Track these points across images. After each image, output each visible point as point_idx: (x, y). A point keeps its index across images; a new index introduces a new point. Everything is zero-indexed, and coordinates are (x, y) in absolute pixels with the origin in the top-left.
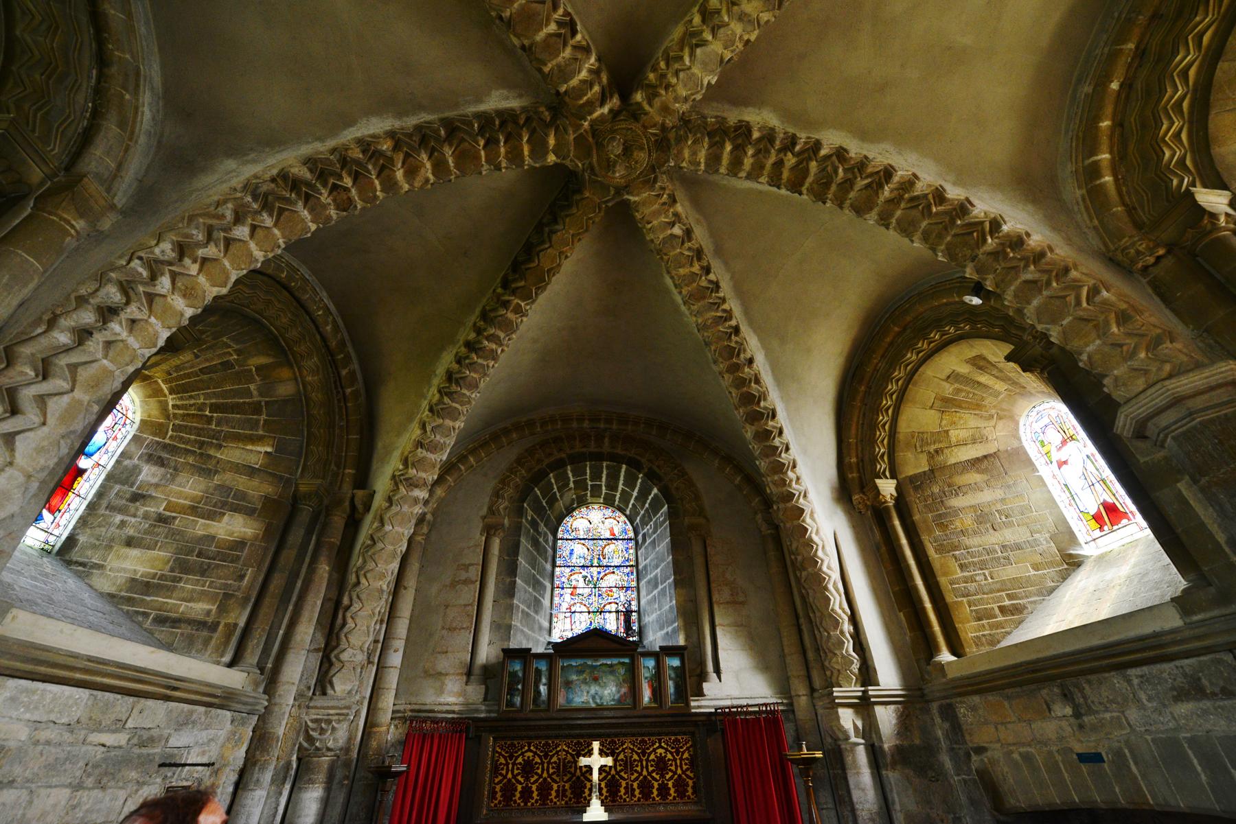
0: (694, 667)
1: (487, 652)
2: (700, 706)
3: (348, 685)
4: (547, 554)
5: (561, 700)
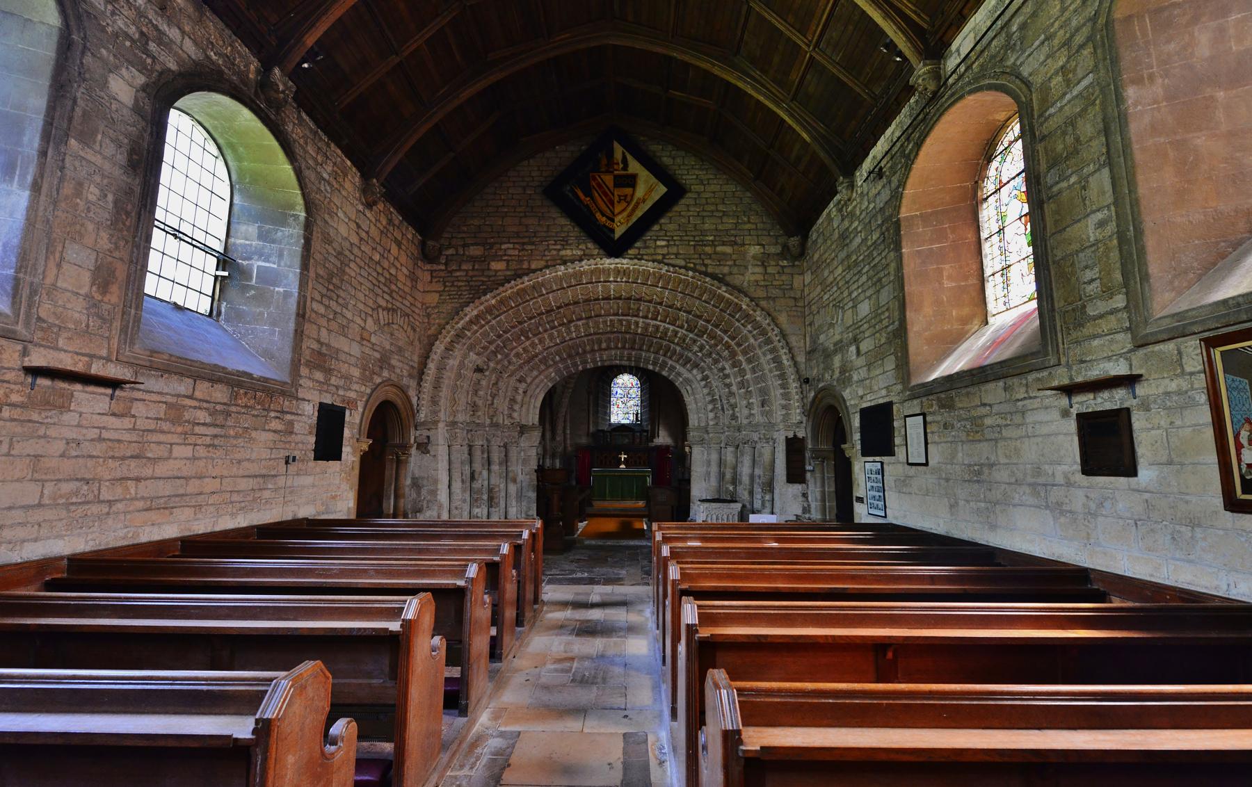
0: (654, 435)
1: (592, 429)
2: (653, 445)
4: (608, 394)
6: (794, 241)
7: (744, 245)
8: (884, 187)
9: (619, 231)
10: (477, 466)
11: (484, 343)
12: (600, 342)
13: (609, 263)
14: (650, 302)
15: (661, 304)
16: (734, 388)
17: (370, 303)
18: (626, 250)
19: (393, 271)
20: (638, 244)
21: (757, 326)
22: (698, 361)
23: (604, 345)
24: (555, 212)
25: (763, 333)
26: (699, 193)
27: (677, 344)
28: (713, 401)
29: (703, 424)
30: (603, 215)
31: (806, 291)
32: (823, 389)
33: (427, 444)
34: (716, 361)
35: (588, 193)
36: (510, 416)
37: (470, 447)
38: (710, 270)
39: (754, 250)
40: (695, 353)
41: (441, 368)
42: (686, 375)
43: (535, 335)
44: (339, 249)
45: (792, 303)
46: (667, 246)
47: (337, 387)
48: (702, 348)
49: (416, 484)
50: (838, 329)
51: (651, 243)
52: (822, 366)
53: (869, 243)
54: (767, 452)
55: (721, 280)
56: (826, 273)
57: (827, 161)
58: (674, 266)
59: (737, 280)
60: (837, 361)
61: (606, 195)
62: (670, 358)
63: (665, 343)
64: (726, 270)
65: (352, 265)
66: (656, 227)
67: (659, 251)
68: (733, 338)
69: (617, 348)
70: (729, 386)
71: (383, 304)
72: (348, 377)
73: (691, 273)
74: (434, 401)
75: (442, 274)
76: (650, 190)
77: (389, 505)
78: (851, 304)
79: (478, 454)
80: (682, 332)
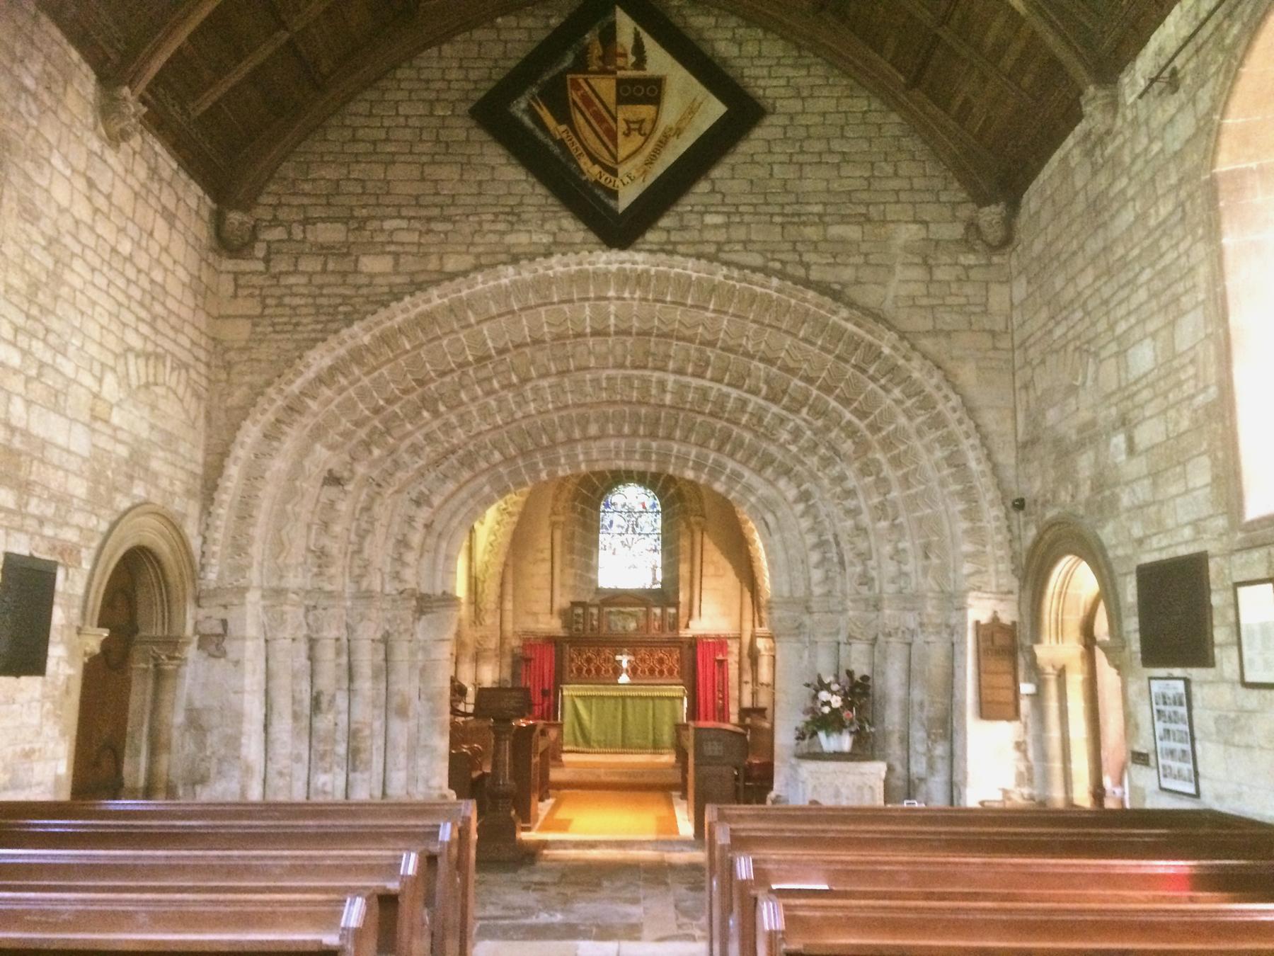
2: (685, 633)
3: (490, 620)
5: (605, 629)
6: (991, 215)
7: (884, 222)
8: (1181, 109)
9: (627, 196)
10: (326, 681)
11: (345, 424)
12: (584, 422)
13: (607, 260)
14: (691, 340)
15: (712, 344)
16: (865, 519)
17: (111, 341)
18: (641, 232)
19: (158, 275)
20: (665, 222)
21: (912, 390)
22: (789, 463)
23: (593, 430)
24: (494, 154)
25: (927, 403)
26: (792, 117)
27: (746, 427)
28: (821, 544)
29: (800, 592)
30: (595, 160)
31: (1017, 318)
32: (1052, 524)
33: (223, 635)
34: (826, 462)
35: (563, 116)
36: (397, 576)
37: (312, 643)
38: (815, 275)
39: (907, 233)
40: (782, 446)
41: (253, 477)
42: (763, 490)
43: (451, 408)
44: (50, 232)
45: (987, 341)
46: (727, 225)
47: (41, 521)
48: (797, 434)
49: (195, 723)
50: (1086, 398)
51: (692, 220)
52: (1052, 474)
53: (1152, 222)
54: (937, 653)
55: (837, 296)
56: (1059, 282)
57: (1063, 53)
58: (741, 267)
59: (870, 296)
60: (1085, 464)
61: (601, 120)
62: (732, 455)
63: (720, 424)
64: (847, 274)
65: (78, 265)
66: (703, 187)
67: (709, 235)
68: (862, 415)
69: (619, 434)
70: (854, 513)
71: (137, 343)
72: (62, 499)
73: (775, 282)
74: (239, 547)
75: (257, 280)
76: (692, 111)
77: (135, 768)
78: (1113, 347)
79: (327, 653)
80: (754, 401)
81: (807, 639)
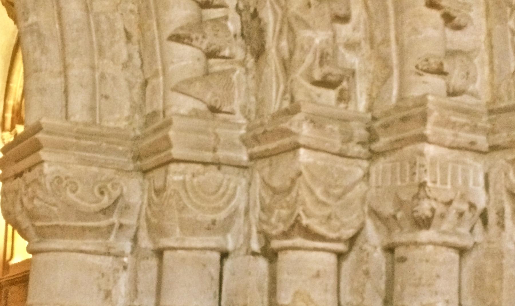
81: (127, 246)
